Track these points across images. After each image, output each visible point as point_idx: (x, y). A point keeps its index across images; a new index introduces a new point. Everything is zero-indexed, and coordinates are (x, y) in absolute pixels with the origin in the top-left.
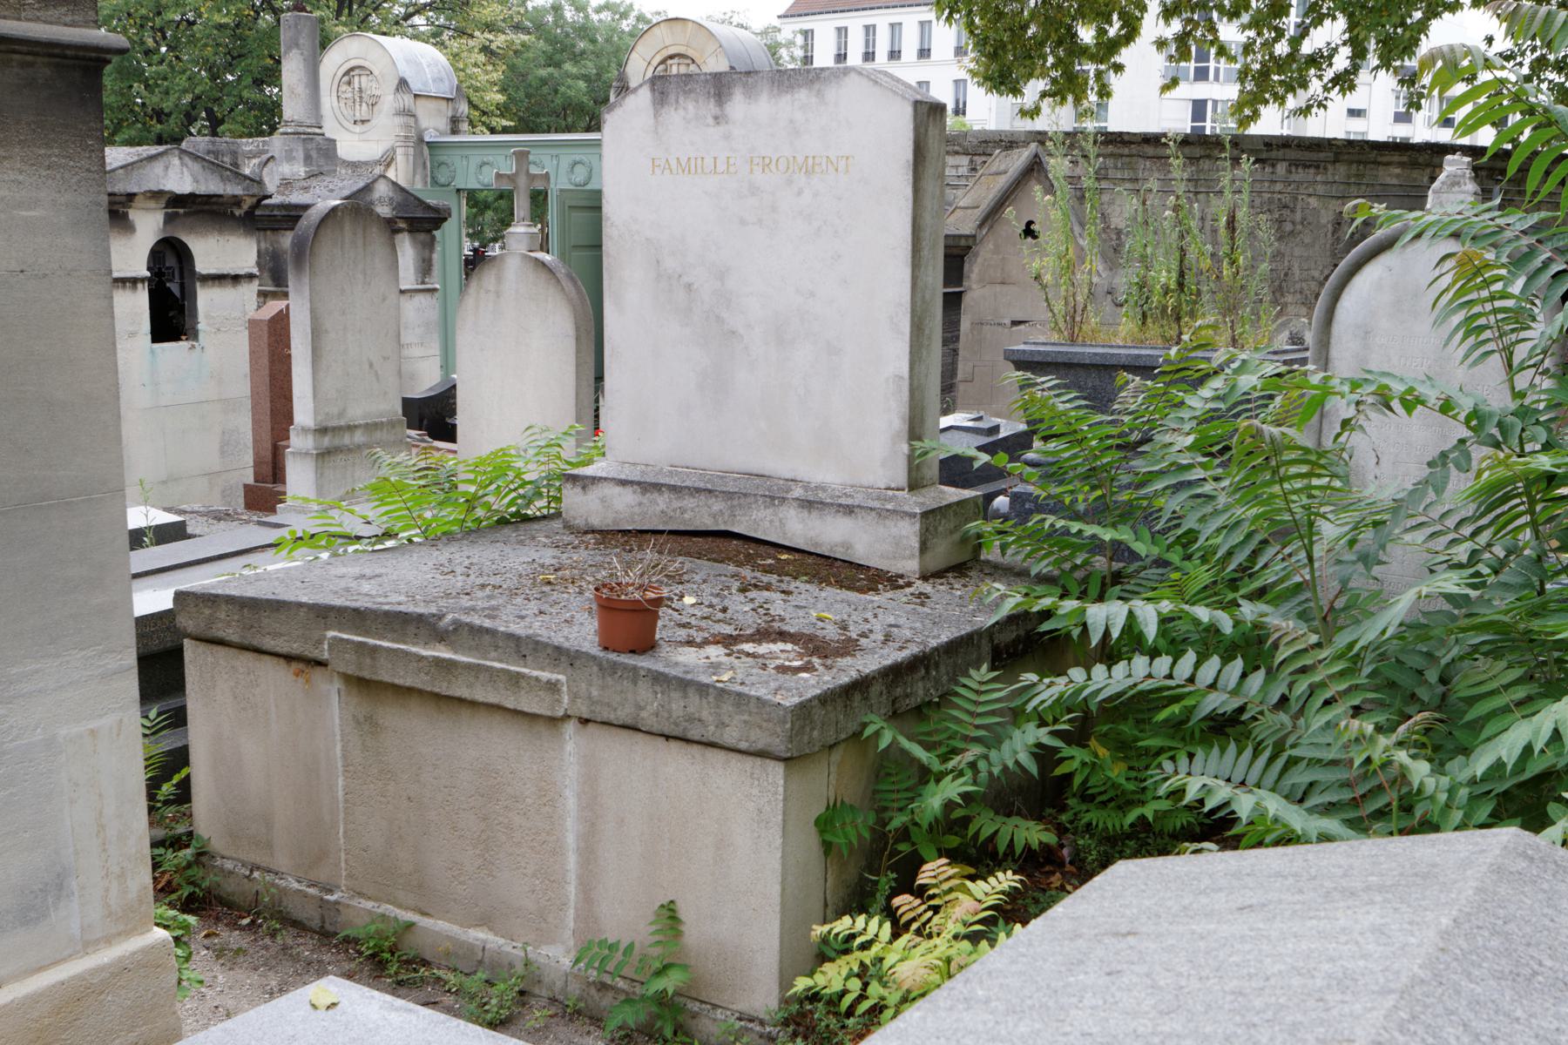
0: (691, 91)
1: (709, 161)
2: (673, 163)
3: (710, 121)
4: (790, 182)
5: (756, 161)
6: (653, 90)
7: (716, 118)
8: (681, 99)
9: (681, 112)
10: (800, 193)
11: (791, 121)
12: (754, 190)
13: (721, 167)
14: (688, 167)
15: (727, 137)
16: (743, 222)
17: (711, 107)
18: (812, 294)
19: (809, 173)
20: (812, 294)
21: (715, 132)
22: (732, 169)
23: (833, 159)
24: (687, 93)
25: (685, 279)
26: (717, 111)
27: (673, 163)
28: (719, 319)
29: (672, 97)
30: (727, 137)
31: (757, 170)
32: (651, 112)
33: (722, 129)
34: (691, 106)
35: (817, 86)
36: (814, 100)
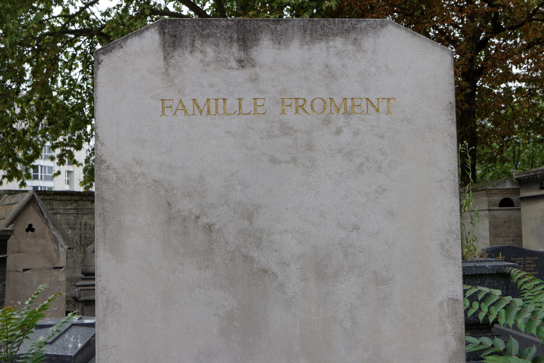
0: (209, 35)
1: (232, 103)
2: (189, 105)
3: (234, 64)
4: (327, 122)
5: (288, 102)
6: (162, 33)
7: (240, 61)
8: (198, 43)
9: (198, 55)
10: (338, 132)
11: (327, 66)
12: (286, 130)
13: (246, 108)
14: (202, 109)
15: (254, 80)
16: (274, 161)
17: (235, 50)
18: (356, 228)
19: (347, 114)
20: (356, 228)
21: (240, 75)
22: (260, 110)
23: (375, 102)
24: (205, 37)
25: (204, 220)
26: (242, 55)
27: (189, 105)
28: (248, 259)
29: (187, 41)
30: (254, 80)
31: (290, 113)
32: (161, 54)
33: (248, 72)
34: (210, 51)
35: (353, 35)
36: (350, 47)
